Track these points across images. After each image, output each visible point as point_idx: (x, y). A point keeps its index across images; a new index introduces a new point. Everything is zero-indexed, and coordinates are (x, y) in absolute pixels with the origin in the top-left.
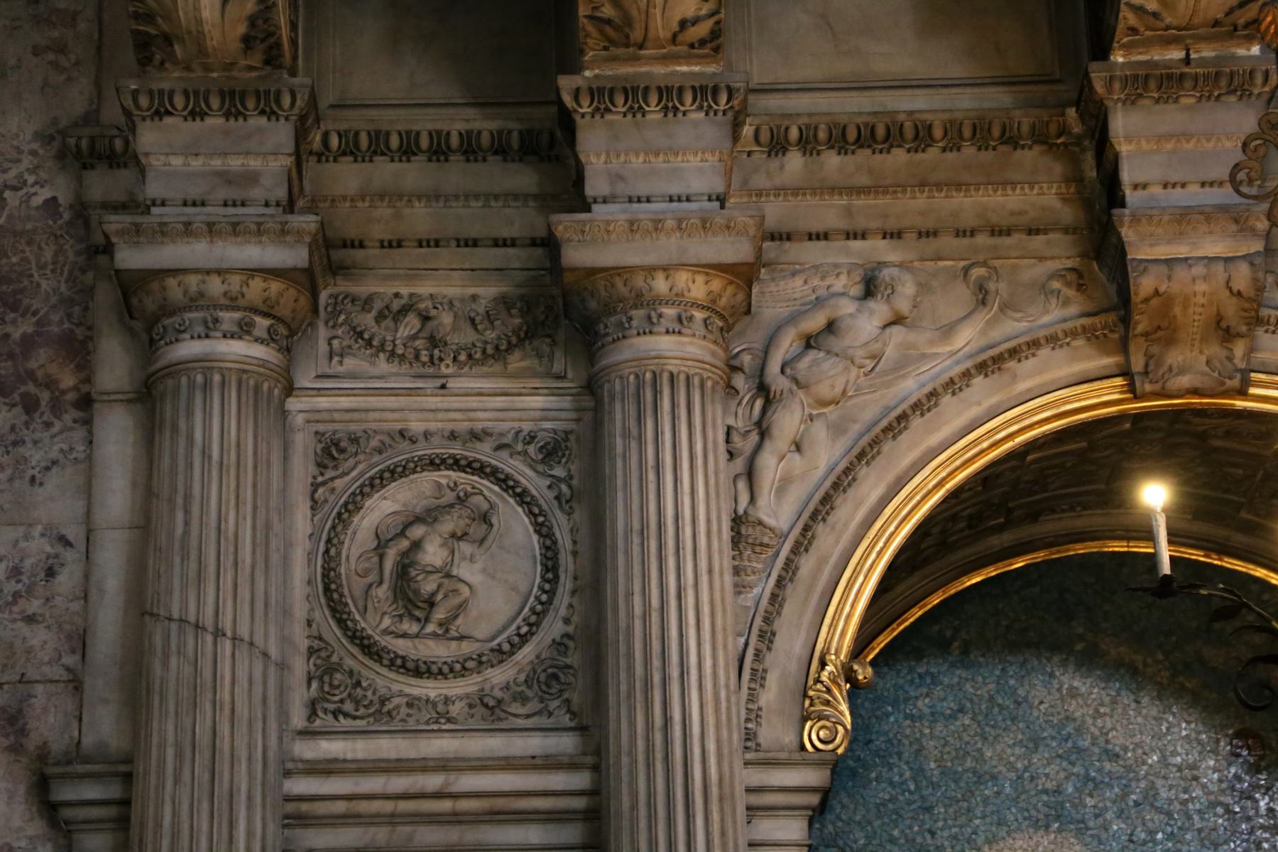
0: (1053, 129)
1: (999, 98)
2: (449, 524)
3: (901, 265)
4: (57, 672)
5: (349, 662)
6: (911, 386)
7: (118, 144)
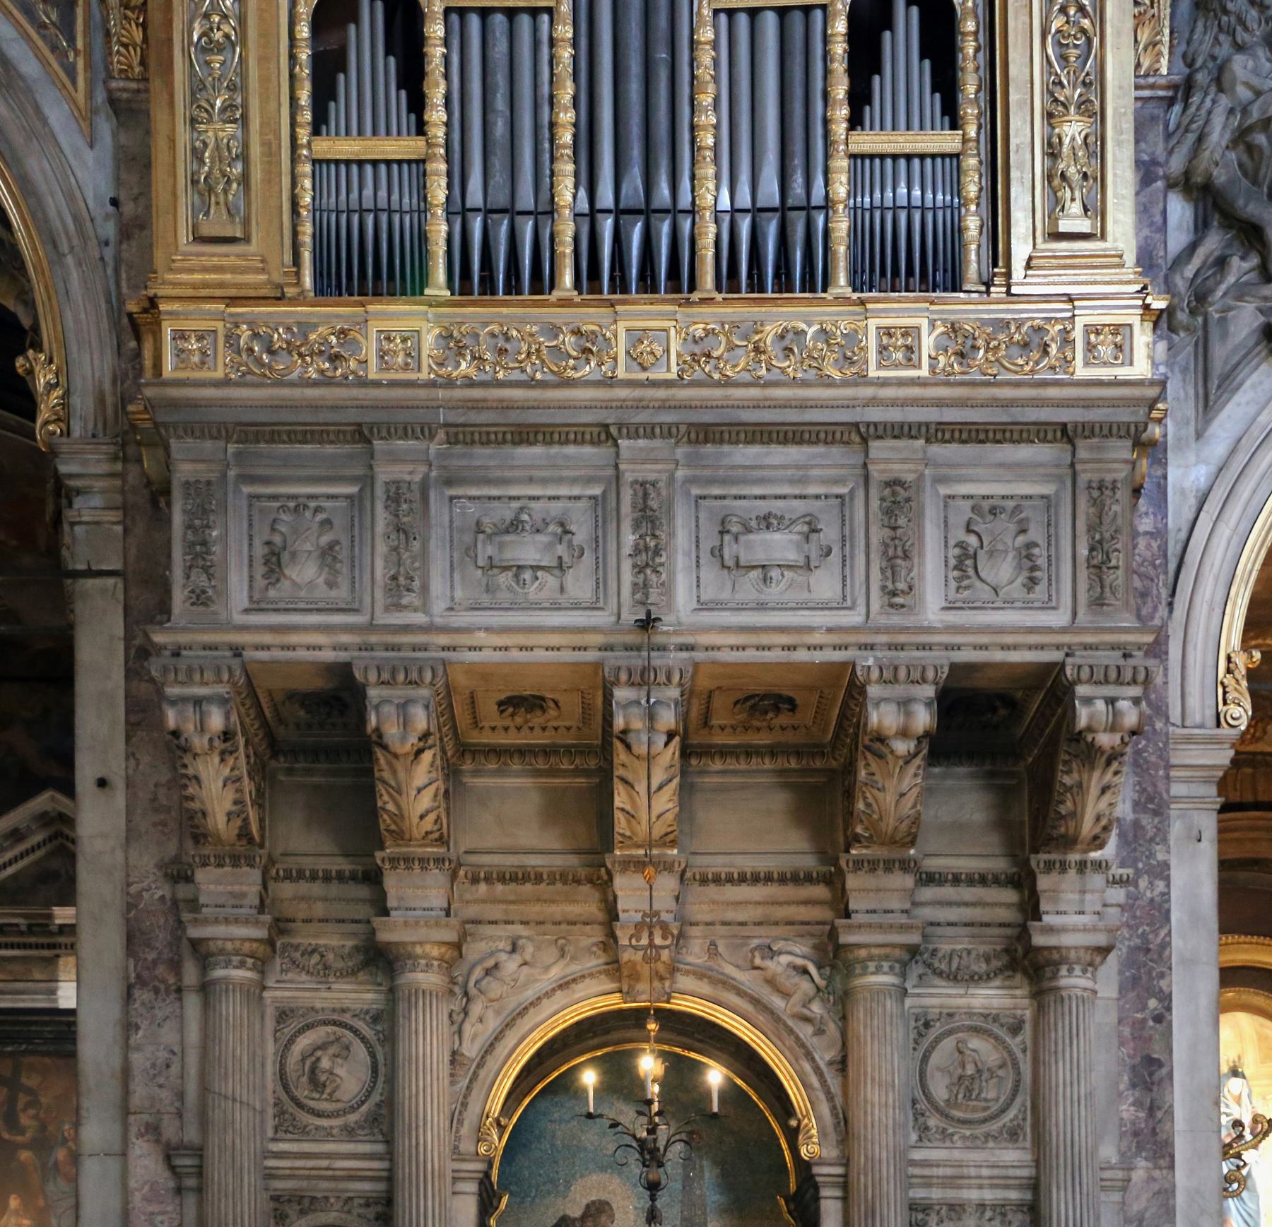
0: (595, 877)
1: (572, 861)
2: (331, 1051)
3: (528, 938)
4: (173, 1110)
5: (291, 1110)
6: (530, 994)
7: (189, 873)
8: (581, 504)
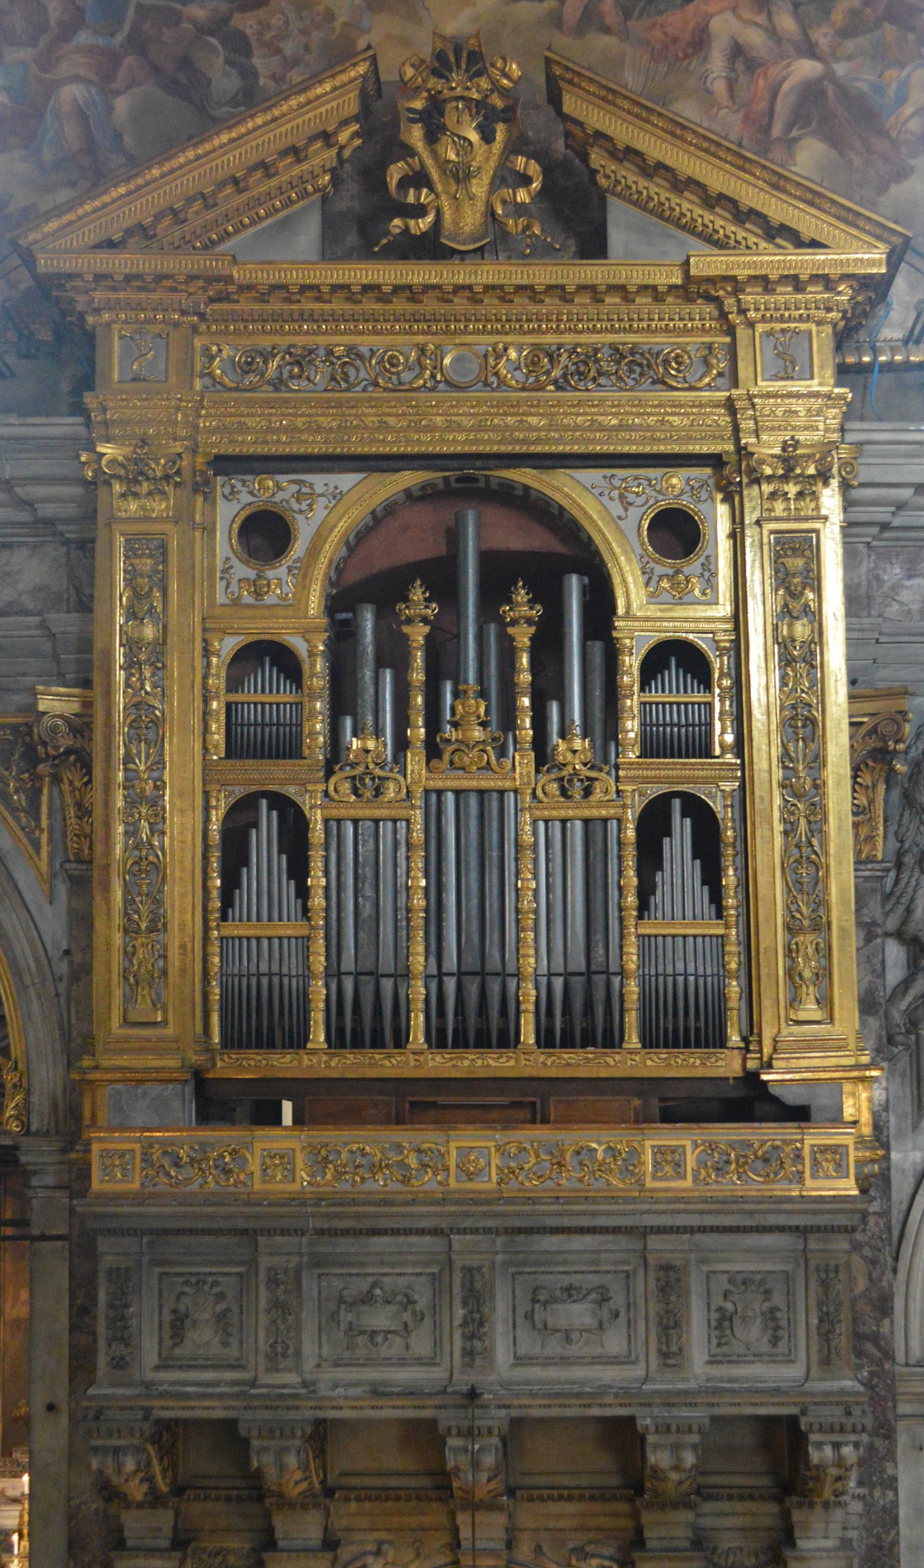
8: (423, 1279)
